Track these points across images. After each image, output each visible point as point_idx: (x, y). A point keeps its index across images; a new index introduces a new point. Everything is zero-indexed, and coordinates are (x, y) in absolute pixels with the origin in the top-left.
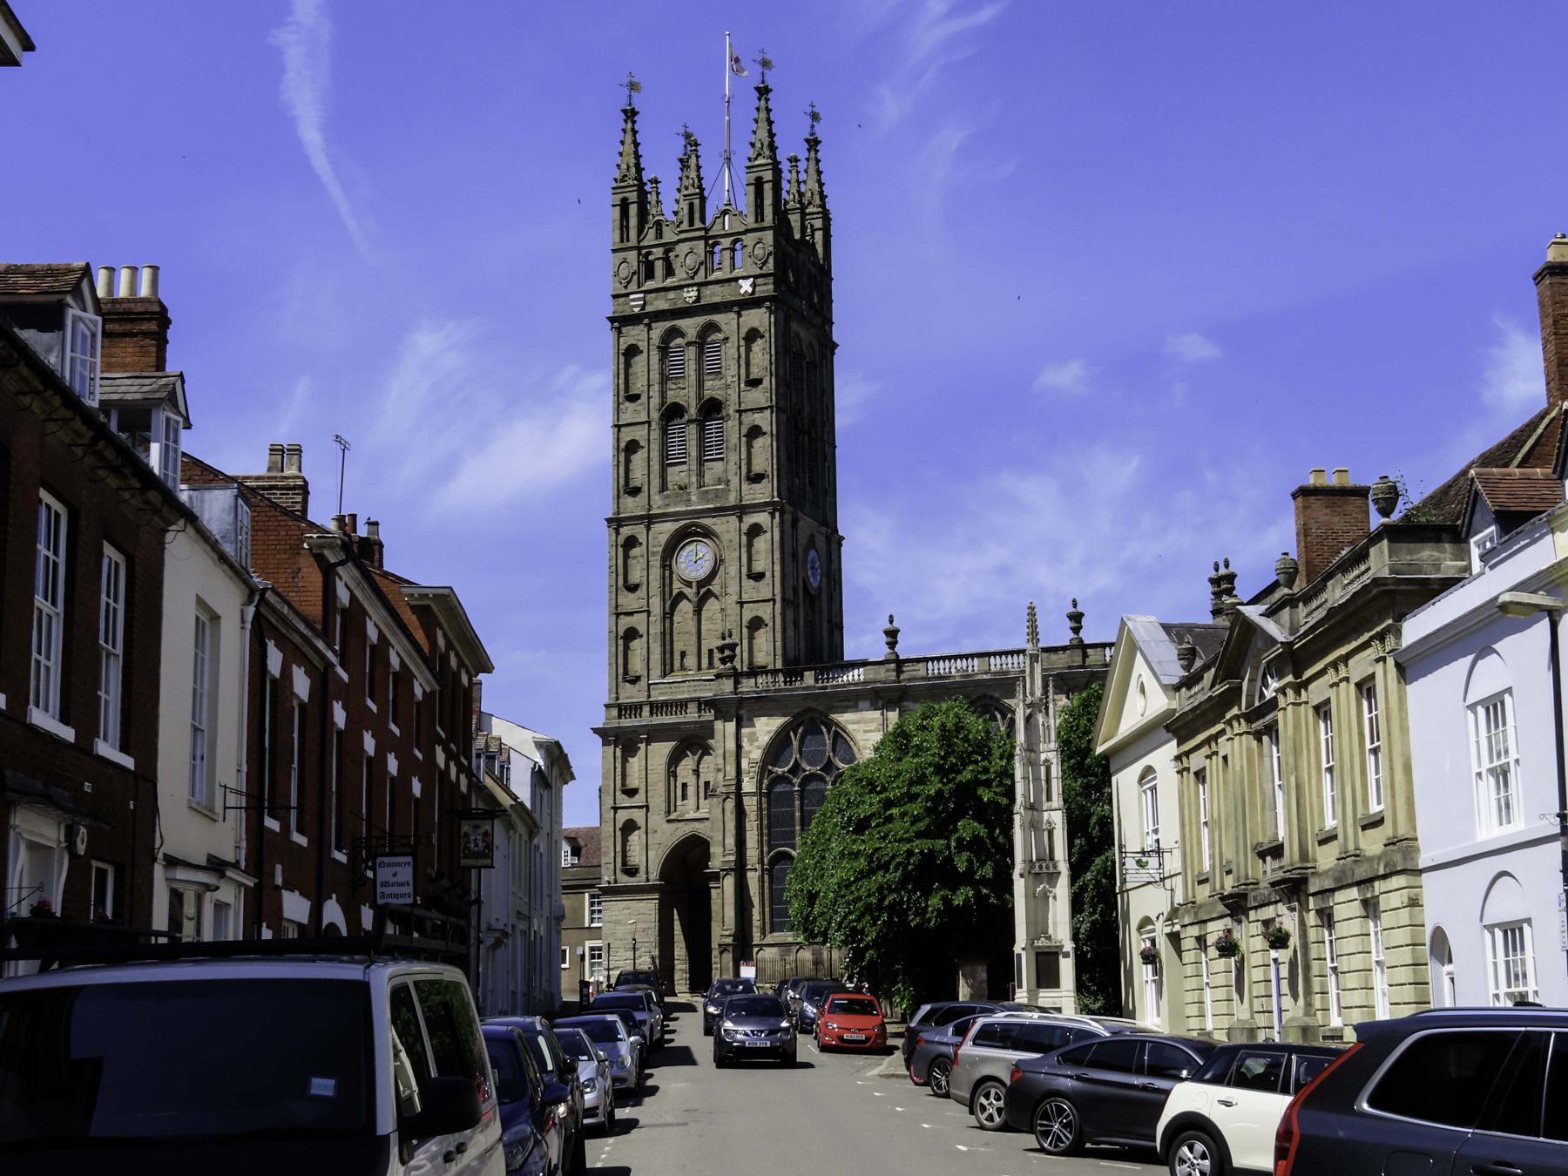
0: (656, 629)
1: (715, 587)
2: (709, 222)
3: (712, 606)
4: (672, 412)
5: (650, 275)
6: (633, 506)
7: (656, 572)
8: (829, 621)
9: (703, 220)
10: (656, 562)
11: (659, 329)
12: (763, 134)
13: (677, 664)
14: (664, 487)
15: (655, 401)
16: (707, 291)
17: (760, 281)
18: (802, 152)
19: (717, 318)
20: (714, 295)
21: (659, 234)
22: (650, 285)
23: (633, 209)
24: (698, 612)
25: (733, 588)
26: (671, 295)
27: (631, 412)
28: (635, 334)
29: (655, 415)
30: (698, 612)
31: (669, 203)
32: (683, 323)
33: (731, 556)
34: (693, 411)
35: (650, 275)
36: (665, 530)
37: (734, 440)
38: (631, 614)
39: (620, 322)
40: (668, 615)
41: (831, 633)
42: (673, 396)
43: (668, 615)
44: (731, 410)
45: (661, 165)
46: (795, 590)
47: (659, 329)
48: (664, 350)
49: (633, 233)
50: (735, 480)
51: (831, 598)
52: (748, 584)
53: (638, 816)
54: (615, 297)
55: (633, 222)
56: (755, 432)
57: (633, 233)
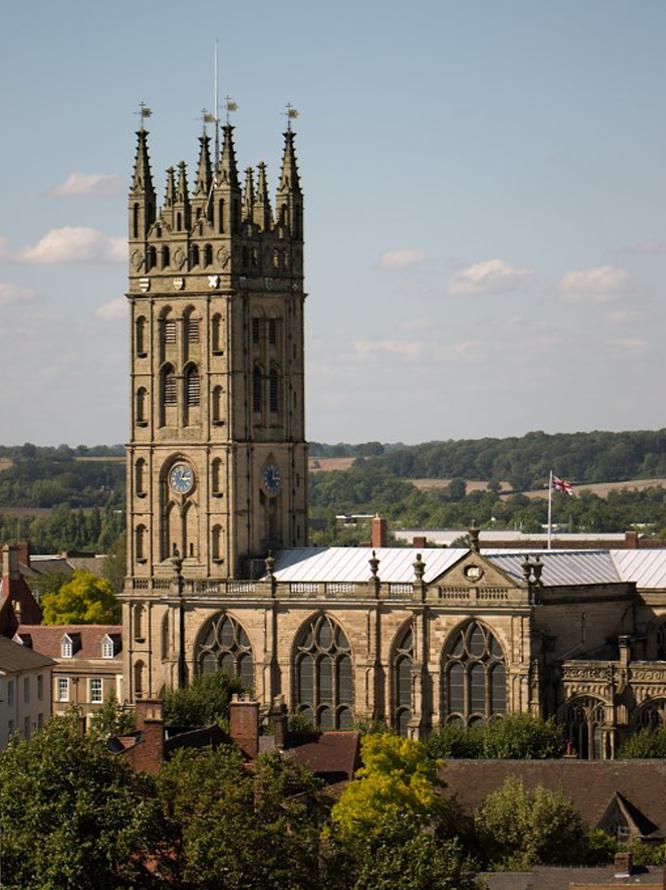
0: (157, 527)
1: (194, 497)
3: (192, 512)
4: (167, 369)
5: (154, 264)
6: (143, 435)
7: (156, 486)
10: (156, 478)
11: (160, 304)
13: (171, 553)
14: (163, 424)
15: (157, 360)
16: (189, 280)
17: (222, 278)
20: (193, 284)
21: (159, 234)
22: (154, 271)
23: (142, 212)
24: (184, 516)
25: (203, 503)
26: (166, 281)
27: (143, 366)
29: (157, 371)
30: (184, 516)
33: (203, 479)
34: (179, 370)
35: (154, 264)
36: (161, 455)
37: (206, 394)
38: (141, 514)
39: (134, 298)
40: (165, 517)
43: (165, 517)
44: (203, 371)
47: (160, 304)
48: (163, 321)
49: (141, 231)
50: (206, 423)
52: (213, 500)
53: (145, 658)
54: (131, 278)
55: (142, 222)
56: (218, 389)
57: (141, 231)
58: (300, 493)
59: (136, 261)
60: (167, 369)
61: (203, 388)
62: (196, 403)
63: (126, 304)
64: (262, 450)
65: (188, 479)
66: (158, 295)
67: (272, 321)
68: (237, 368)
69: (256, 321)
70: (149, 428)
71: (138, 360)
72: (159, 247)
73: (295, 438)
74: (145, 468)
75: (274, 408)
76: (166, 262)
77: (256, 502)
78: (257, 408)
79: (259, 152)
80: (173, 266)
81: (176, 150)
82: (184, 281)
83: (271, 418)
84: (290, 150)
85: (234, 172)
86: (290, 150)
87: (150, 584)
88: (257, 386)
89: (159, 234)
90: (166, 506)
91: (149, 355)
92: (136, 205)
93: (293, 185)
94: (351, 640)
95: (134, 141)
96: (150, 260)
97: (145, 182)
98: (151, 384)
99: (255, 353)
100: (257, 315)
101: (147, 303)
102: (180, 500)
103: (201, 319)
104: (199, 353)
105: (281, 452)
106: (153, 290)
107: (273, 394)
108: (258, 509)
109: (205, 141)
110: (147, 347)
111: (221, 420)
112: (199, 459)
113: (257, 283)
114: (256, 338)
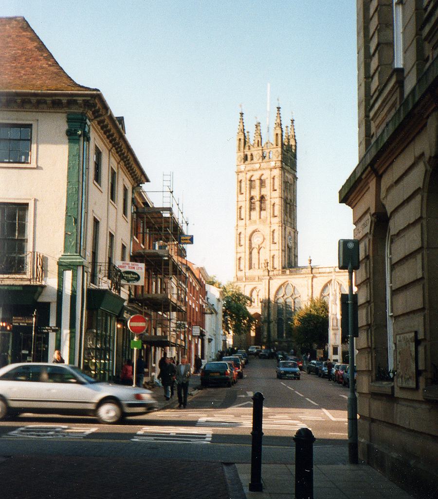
1: (263, 245)
2: (263, 145)
6: (242, 223)
8: (294, 255)
9: (261, 145)
11: (249, 174)
12: (278, 121)
13: (253, 267)
16: (262, 164)
18: (290, 124)
19: (263, 172)
21: (249, 149)
22: (247, 162)
27: (242, 197)
28: (242, 176)
31: (252, 139)
36: (250, 230)
39: (238, 173)
41: (295, 258)
42: (252, 194)
44: (267, 198)
45: (250, 128)
46: (285, 247)
51: (295, 248)
52: (272, 245)
57: (242, 148)
59: (239, 159)
61: (268, 204)
62: (264, 210)
63: (235, 175)
65: (261, 240)
66: (249, 171)
68: (283, 197)
70: (244, 195)
71: (240, 196)
72: (249, 154)
74: (242, 236)
76: (252, 159)
80: (255, 160)
82: (260, 165)
87: (244, 279)
89: (249, 149)
90: (251, 249)
91: (244, 194)
92: (240, 139)
96: (246, 158)
98: (246, 205)
101: (244, 174)
102: (257, 247)
103: (267, 178)
104: (266, 191)
106: (247, 169)
110: (242, 243)
111: (276, 215)
112: (266, 231)
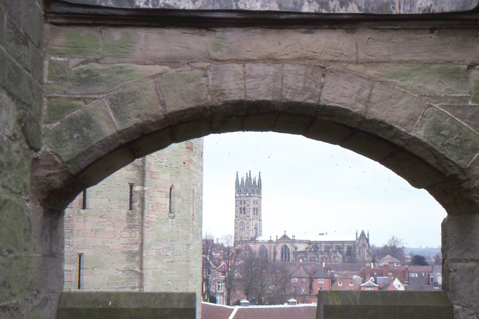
32: (242, 198)
39: (236, 197)
58: (261, 228)
60: (241, 208)
64: (255, 221)
67: (257, 201)
69: (254, 201)
73: (260, 220)
75: (257, 214)
76: (241, 192)
77: (254, 228)
78: (254, 214)
79: (254, 175)
81: (242, 175)
83: (256, 216)
84: (260, 175)
85: (250, 178)
86: (260, 175)
88: (254, 211)
93: (260, 180)
94: (267, 249)
95: (236, 173)
97: (237, 180)
98: (239, 211)
99: (254, 206)
100: (254, 200)
105: (258, 222)
107: (257, 212)
108: (254, 231)
109: (247, 174)
113: (254, 195)
114: (254, 203)
